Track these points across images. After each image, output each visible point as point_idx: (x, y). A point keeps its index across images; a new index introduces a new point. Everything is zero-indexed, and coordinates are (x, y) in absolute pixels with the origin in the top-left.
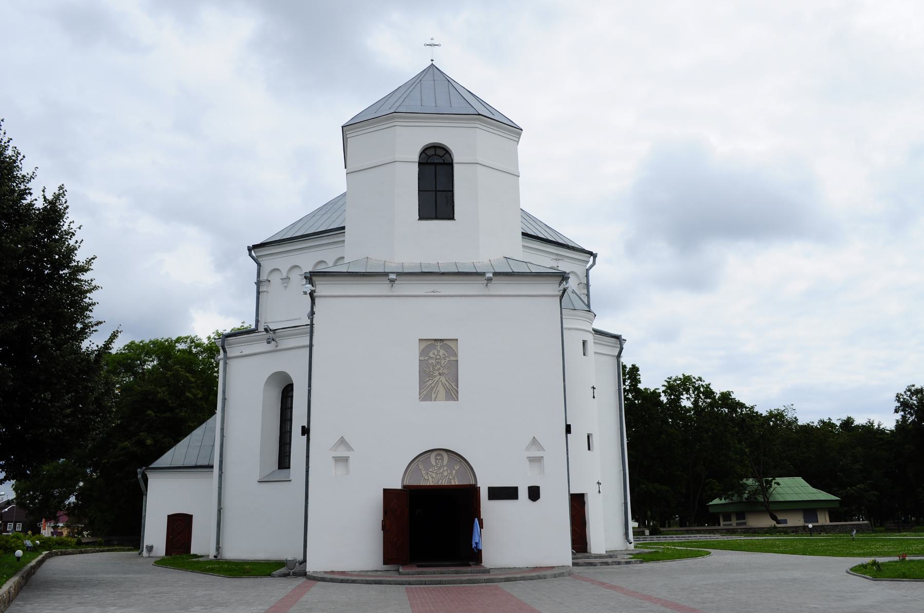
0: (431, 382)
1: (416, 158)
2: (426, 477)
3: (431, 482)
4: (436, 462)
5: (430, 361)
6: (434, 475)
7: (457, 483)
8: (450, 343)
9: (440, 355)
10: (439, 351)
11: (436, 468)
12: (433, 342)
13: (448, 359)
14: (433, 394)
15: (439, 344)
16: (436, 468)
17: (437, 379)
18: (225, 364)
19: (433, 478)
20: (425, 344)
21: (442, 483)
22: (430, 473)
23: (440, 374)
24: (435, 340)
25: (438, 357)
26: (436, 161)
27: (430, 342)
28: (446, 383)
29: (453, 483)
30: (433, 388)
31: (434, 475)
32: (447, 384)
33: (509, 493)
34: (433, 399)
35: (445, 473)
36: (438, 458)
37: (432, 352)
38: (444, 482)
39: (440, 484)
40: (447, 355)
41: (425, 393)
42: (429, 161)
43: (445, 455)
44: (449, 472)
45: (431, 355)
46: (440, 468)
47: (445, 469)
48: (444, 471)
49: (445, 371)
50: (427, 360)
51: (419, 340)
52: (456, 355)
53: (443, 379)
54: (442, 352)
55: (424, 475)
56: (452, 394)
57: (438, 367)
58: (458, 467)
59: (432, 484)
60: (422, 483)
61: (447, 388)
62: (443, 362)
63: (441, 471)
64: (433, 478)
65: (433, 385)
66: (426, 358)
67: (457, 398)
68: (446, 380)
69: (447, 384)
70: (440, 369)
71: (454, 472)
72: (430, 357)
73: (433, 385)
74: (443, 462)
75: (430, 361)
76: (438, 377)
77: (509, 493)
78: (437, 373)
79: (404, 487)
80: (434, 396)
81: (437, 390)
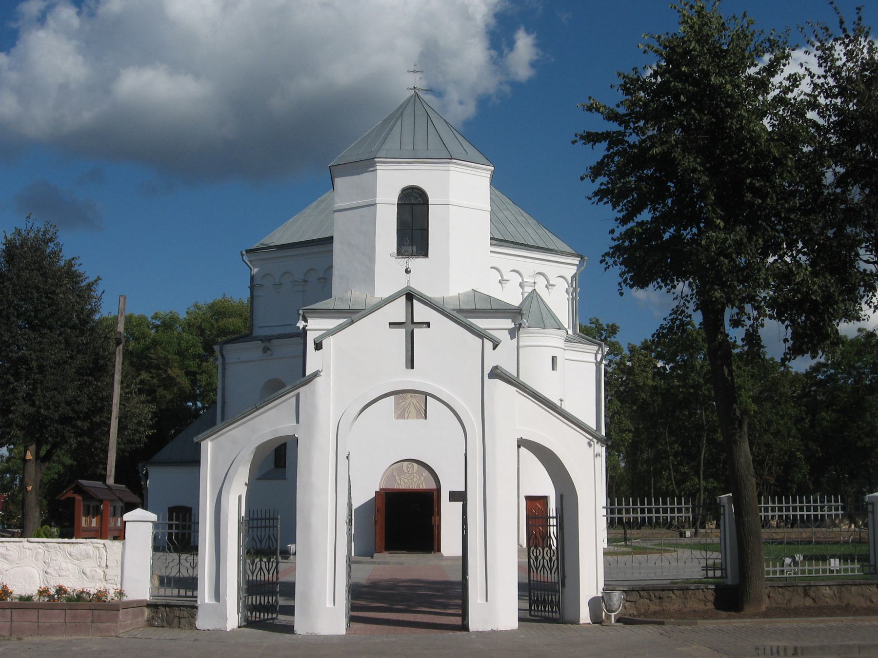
0: (404, 403)
1: (395, 200)
2: (399, 482)
6: (406, 480)
7: (424, 488)
14: (406, 413)
17: (408, 401)
18: (224, 369)
19: (405, 483)
26: (413, 202)
28: (416, 403)
29: (421, 488)
32: (418, 405)
35: (415, 479)
38: (414, 486)
39: (411, 488)
42: (406, 202)
43: (415, 465)
46: (411, 474)
59: (404, 488)
60: (396, 487)
63: (412, 477)
64: (405, 483)
65: (406, 406)
69: (418, 405)
71: (422, 478)
73: (406, 406)
76: (410, 399)
79: (381, 489)
80: (406, 415)
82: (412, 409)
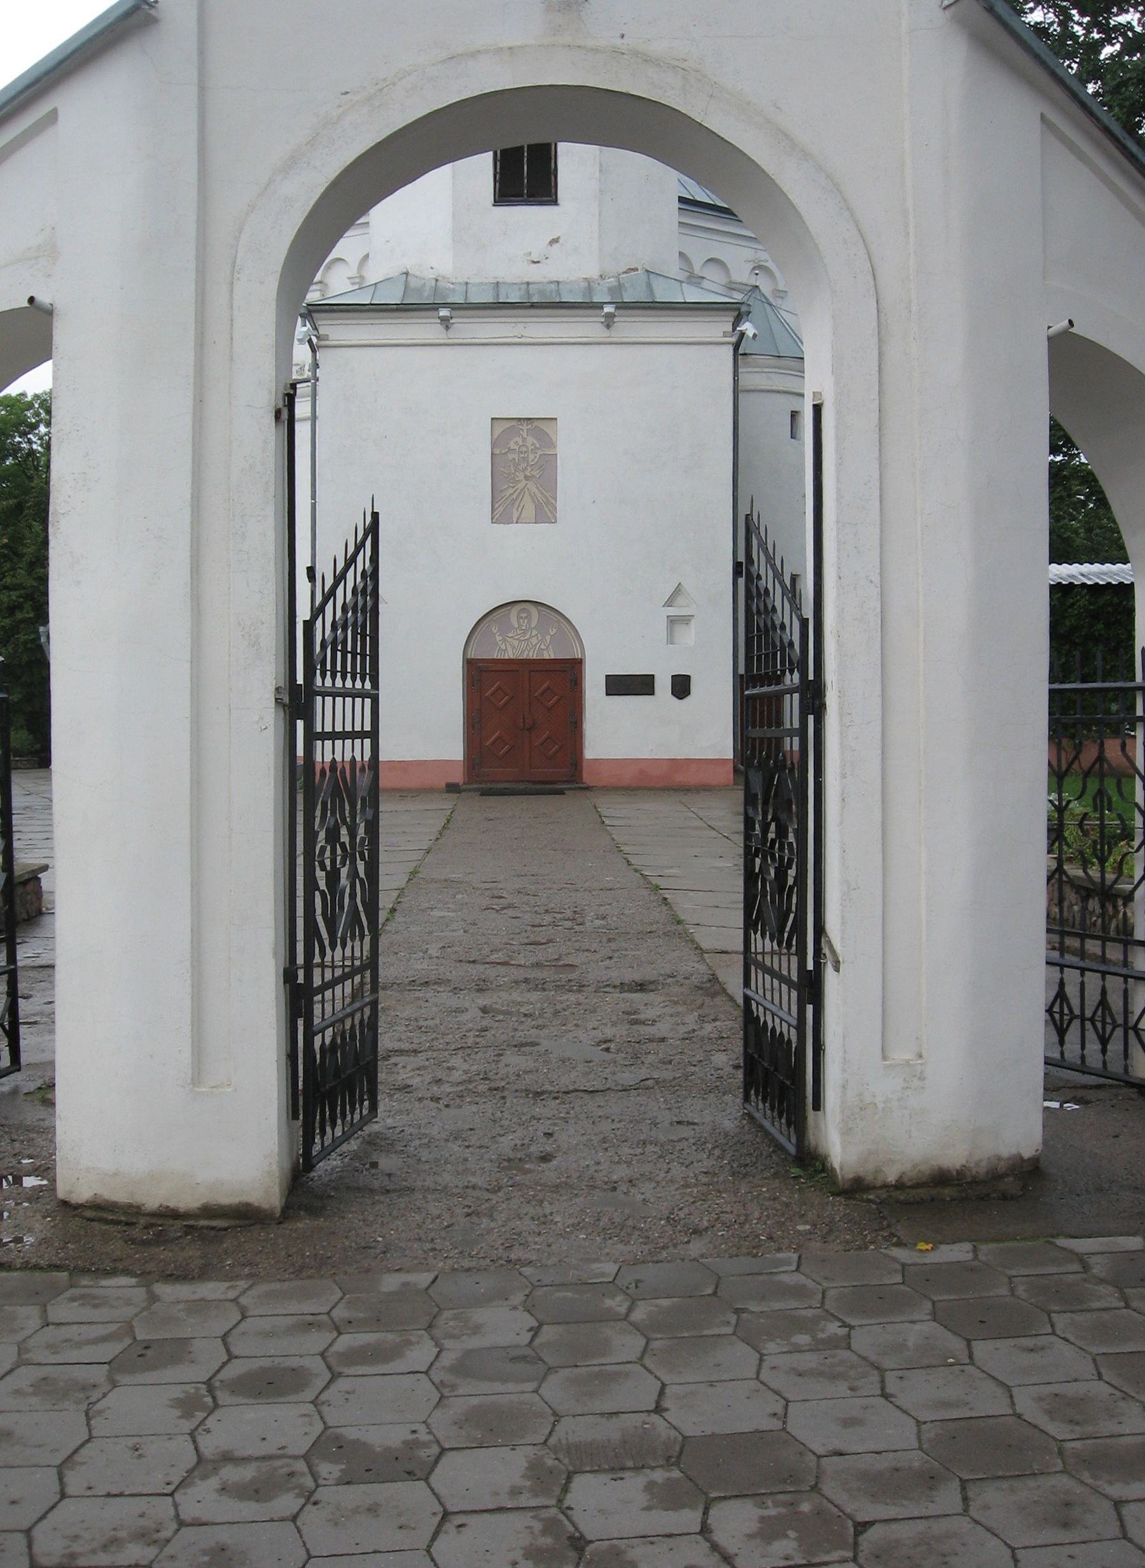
0: (511, 491)
3: (510, 655)
4: (518, 622)
5: (510, 456)
6: (516, 643)
8: (543, 426)
9: (527, 448)
10: (524, 439)
11: (519, 632)
12: (514, 423)
13: (540, 452)
14: (515, 511)
16: (519, 632)
17: (520, 486)
20: (500, 428)
21: (528, 655)
22: (510, 640)
23: (526, 478)
24: (520, 419)
25: (524, 449)
27: (508, 424)
31: (516, 643)
32: (539, 495)
33: (641, 685)
34: (515, 520)
35: (534, 641)
36: (524, 615)
37: (515, 440)
39: (525, 657)
40: (538, 446)
41: (501, 509)
43: (533, 610)
44: (540, 638)
45: (512, 445)
47: (534, 632)
48: (531, 637)
49: (535, 473)
50: (506, 453)
51: (492, 419)
52: (553, 445)
54: (530, 440)
55: (500, 643)
56: (545, 513)
57: (523, 465)
58: (555, 631)
59: (511, 657)
60: (496, 655)
61: (538, 501)
62: (531, 457)
65: (514, 496)
67: (555, 518)
68: (537, 488)
69: (539, 495)
71: (548, 638)
72: (510, 449)
73: (514, 496)
74: (529, 622)
75: (510, 456)
76: (524, 482)
77: (641, 685)
78: (521, 476)
80: (515, 515)
81: (522, 504)
82: (527, 500)
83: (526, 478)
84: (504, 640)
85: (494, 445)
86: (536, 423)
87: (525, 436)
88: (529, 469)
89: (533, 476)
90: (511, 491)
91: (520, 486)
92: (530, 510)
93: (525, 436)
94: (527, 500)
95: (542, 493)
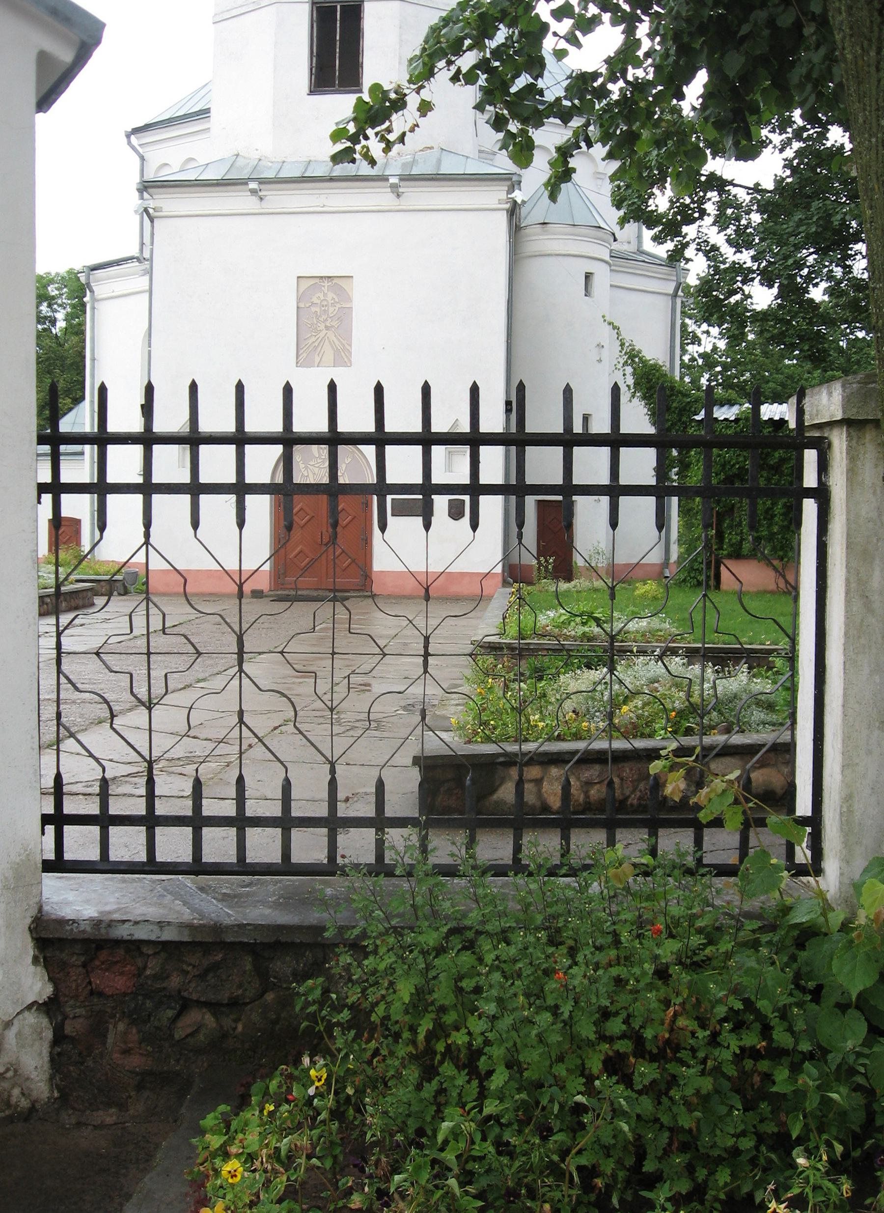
0: (313, 339)
6: (316, 470)
7: (347, 482)
10: (325, 295)
12: (317, 280)
13: (338, 306)
14: (316, 356)
15: (326, 284)
17: (322, 335)
22: (311, 467)
23: (327, 328)
24: (322, 277)
25: (325, 303)
27: (312, 281)
28: (335, 339)
30: (316, 348)
31: (316, 470)
32: (337, 343)
37: (317, 295)
40: (337, 300)
41: (305, 355)
45: (315, 300)
49: (334, 323)
51: (298, 277)
52: (350, 300)
53: (331, 335)
54: (330, 295)
57: (324, 317)
62: (331, 309)
66: (307, 305)
67: (350, 361)
69: (337, 343)
70: (326, 320)
75: (313, 309)
76: (324, 332)
78: (322, 326)
80: (317, 359)
83: (327, 328)
84: (306, 468)
85: (299, 300)
86: (335, 281)
87: (325, 290)
88: (330, 320)
89: (332, 326)
90: (313, 339)
91: (322, 335)
92: (329, 356)
93: (325, 290)
94: (327, 346)
95: (339, 340)
